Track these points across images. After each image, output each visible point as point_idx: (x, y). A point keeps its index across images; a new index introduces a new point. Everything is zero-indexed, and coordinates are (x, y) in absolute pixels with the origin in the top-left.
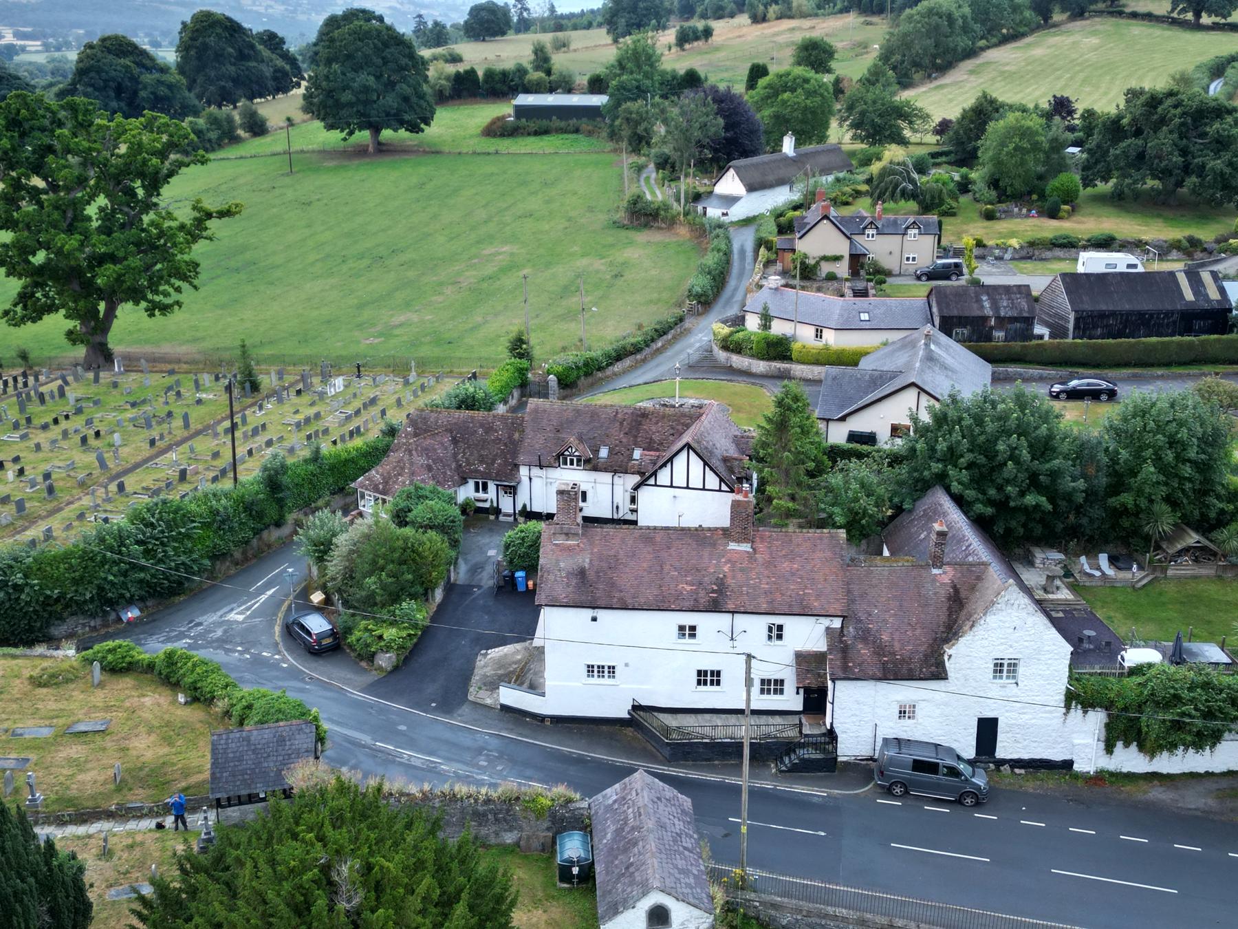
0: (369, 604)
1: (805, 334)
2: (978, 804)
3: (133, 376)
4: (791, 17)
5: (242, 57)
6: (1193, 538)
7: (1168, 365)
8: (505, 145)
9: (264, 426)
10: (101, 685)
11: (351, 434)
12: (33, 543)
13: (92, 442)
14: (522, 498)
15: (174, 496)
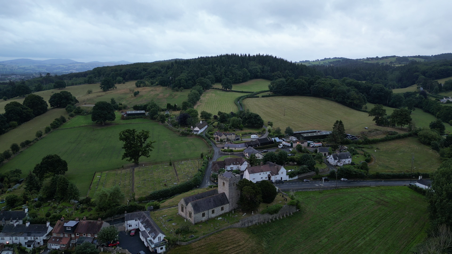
1: (234, 149)
2: (283, 183)
4: (146, 86)
6: (286, 163)
7: (269, 148)
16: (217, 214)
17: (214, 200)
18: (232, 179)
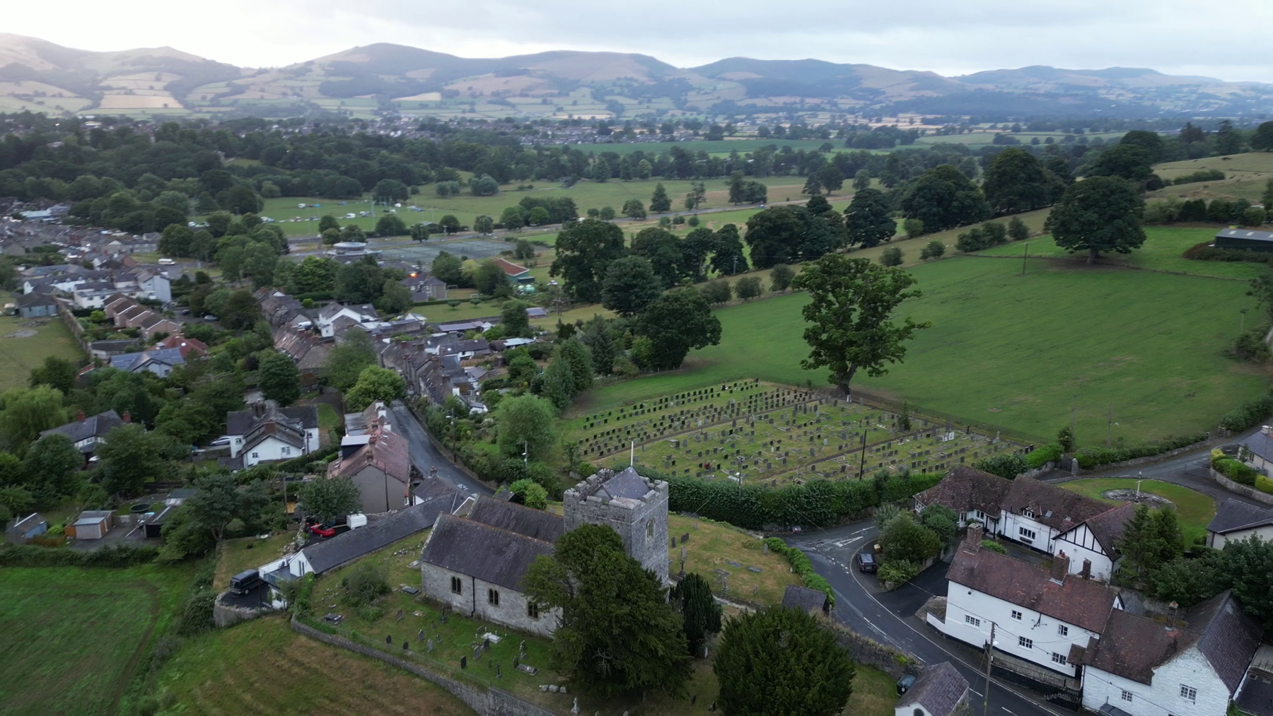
0: (890, 557)
3: (855, 406)
5: (1030, 179)
8: (1200, 268)
9: (896, 452)
10: (766, 554)
11: (937, 467)
12: (766, 485)
13: (816, 440)
14: (1000, 527)
15: (832, 480)
16: (510, 617)
17: (516, 558)
18: (582, 502)
